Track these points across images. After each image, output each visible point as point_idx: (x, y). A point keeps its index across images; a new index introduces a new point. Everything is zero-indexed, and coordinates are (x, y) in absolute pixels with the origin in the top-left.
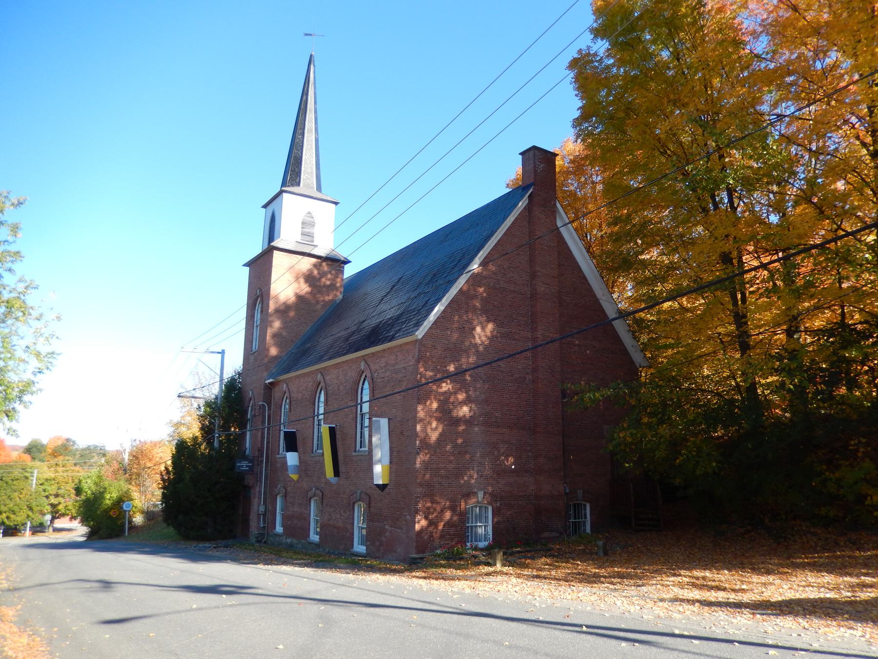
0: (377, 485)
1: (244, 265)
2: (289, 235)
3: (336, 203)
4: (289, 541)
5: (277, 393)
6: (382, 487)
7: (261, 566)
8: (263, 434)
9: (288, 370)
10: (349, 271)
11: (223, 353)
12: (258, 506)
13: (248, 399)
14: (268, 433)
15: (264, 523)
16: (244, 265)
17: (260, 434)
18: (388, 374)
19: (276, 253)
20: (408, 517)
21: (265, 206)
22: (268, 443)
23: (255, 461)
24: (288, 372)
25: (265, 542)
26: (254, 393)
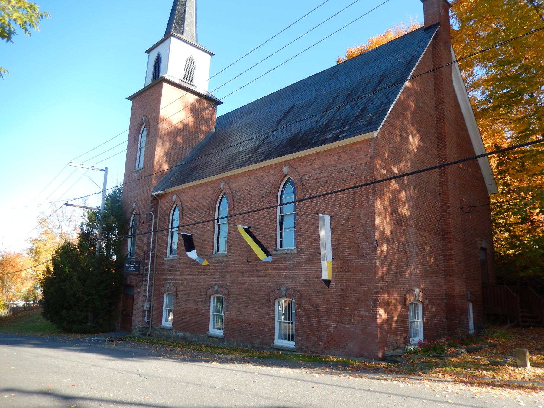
0: (325, 281)
1: (128, 99)
2: (173, 71)
3: (211, 54)
4: (180, 334)
5: (163, 204)
6: (328, 282)
7: (215, 364)
8: (149, 240)
9: (173, 185)
10: (221, 111)
11: (105, 170)
12: (142, 302)
13: (130, 210)
14: (154, 239)
15: (149, 317)
16: (128, 99)
17: (145, 240)
18: (325, 174)
19: (165, 85)
20: (364, 313)
21: (148, 52)
22: (154, 247)
23: (141, 263)
24: (183, 182)
25: (149, 335)
26: (137, 205)
